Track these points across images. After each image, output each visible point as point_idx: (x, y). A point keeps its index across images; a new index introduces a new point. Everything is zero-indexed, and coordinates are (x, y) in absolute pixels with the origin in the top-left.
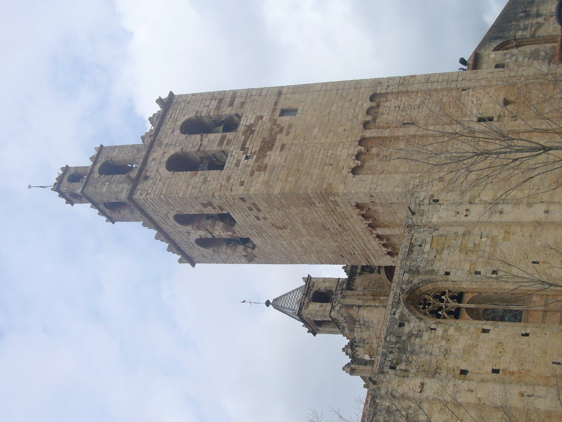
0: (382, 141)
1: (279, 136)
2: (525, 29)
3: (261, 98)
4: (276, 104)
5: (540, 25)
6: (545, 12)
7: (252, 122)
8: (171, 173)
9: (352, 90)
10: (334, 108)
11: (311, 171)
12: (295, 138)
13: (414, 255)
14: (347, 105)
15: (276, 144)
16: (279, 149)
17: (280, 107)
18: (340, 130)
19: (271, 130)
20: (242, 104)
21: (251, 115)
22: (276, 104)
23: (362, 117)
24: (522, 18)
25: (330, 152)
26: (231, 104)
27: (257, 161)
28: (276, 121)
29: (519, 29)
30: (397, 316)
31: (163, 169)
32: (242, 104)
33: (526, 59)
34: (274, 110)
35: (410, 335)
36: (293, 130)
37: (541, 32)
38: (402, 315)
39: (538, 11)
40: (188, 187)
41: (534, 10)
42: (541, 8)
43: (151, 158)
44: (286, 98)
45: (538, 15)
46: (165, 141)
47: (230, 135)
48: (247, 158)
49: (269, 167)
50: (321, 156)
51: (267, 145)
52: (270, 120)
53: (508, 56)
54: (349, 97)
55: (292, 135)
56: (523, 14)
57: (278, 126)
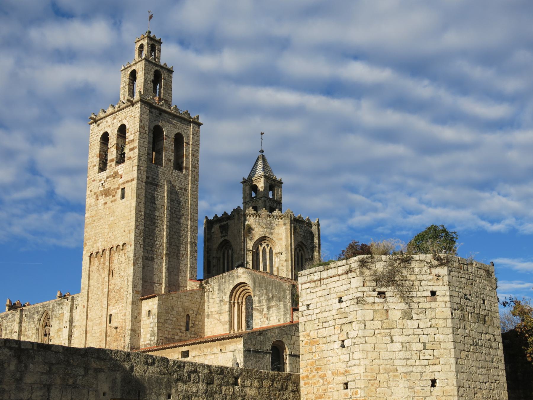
0: (104, 263)
1: (111, 196)
2: (260, 302)
3: (131, 168)
4: (128, 182)
5: (261, 312)
6: (271, 312)
7: (120, 173)
8: (99, 140)
9: (129, 228)
10: (122, 222)
11: (93, 230)
12: (109, 208)
13: (58, 307)
14: (122, 230)
15: (108, 198)
16: (105, 202)
17: (127, 186)
18: (110, 234)
19: (114, 189)
20: (130, 158)
21: (122, 169)
22: (128, 182)
23: (115, 244)
24: (268, 296)
25: (100, 235)
26: (131, 150)
27: (101, 192)
28: (118, 188)
29: (259, 298)
30: (40, 309)
31: (102, 133)
32: (130, 158)
33: (151, 329)
34: (124, 183)
35: (33, 318)
36: (113, 203)
37: (255, 314)
38: (39, 311)
39: (272, 307)
40: (93, 157)
41: (273, 304)
42: (274, 309)
43: (108, 119)
44: (130, 186)
45: (269, 308)
46: (115, 121)
47: (114, 163)
48: (103, 184)
49: (98, 201)
50: (99, 230)
51: (107, 193)
52: (119, 185)
53: (154, 317)
54: (126, 229)
55: (111, 204)
56: (271, 296)
57: (116, 192)
